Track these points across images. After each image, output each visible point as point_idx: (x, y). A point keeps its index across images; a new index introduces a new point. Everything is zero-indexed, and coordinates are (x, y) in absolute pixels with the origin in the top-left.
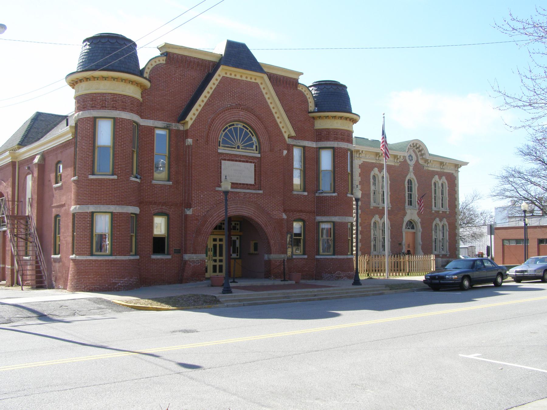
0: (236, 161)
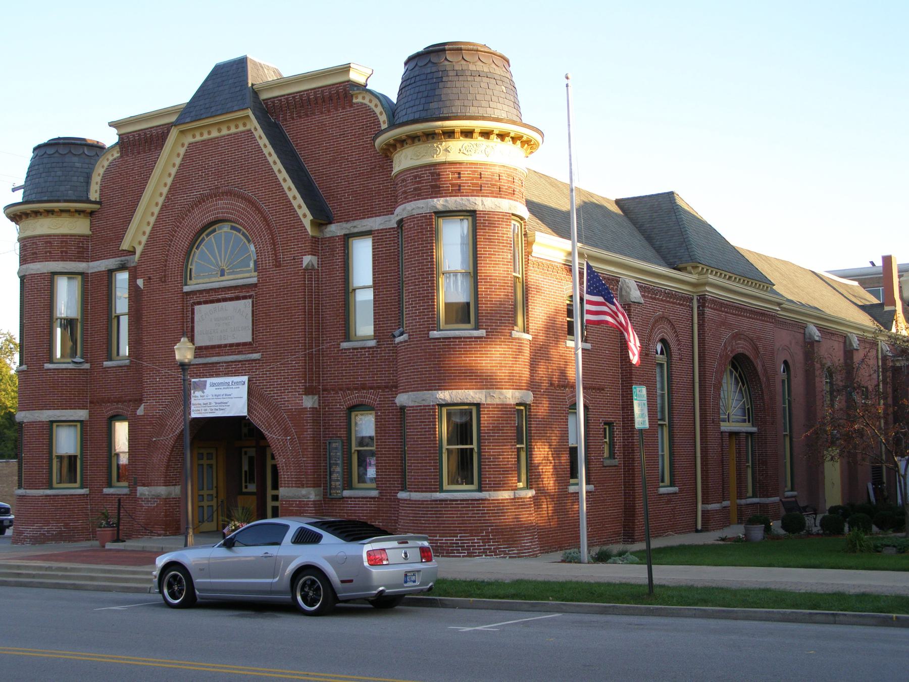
0: (218, 301)
